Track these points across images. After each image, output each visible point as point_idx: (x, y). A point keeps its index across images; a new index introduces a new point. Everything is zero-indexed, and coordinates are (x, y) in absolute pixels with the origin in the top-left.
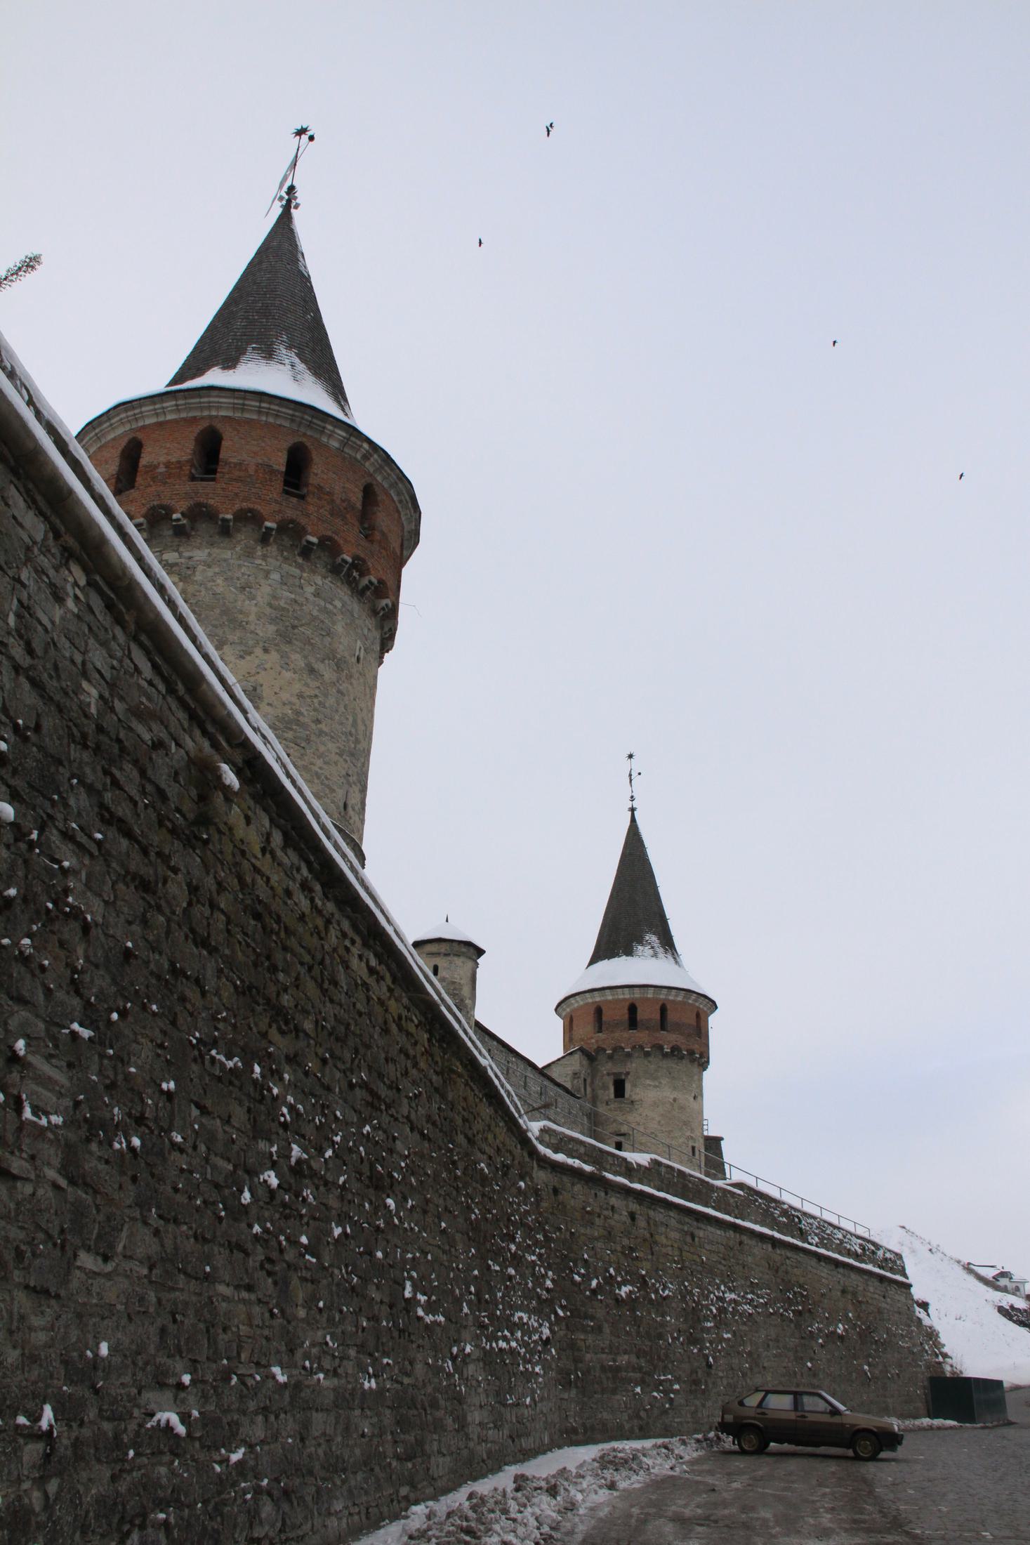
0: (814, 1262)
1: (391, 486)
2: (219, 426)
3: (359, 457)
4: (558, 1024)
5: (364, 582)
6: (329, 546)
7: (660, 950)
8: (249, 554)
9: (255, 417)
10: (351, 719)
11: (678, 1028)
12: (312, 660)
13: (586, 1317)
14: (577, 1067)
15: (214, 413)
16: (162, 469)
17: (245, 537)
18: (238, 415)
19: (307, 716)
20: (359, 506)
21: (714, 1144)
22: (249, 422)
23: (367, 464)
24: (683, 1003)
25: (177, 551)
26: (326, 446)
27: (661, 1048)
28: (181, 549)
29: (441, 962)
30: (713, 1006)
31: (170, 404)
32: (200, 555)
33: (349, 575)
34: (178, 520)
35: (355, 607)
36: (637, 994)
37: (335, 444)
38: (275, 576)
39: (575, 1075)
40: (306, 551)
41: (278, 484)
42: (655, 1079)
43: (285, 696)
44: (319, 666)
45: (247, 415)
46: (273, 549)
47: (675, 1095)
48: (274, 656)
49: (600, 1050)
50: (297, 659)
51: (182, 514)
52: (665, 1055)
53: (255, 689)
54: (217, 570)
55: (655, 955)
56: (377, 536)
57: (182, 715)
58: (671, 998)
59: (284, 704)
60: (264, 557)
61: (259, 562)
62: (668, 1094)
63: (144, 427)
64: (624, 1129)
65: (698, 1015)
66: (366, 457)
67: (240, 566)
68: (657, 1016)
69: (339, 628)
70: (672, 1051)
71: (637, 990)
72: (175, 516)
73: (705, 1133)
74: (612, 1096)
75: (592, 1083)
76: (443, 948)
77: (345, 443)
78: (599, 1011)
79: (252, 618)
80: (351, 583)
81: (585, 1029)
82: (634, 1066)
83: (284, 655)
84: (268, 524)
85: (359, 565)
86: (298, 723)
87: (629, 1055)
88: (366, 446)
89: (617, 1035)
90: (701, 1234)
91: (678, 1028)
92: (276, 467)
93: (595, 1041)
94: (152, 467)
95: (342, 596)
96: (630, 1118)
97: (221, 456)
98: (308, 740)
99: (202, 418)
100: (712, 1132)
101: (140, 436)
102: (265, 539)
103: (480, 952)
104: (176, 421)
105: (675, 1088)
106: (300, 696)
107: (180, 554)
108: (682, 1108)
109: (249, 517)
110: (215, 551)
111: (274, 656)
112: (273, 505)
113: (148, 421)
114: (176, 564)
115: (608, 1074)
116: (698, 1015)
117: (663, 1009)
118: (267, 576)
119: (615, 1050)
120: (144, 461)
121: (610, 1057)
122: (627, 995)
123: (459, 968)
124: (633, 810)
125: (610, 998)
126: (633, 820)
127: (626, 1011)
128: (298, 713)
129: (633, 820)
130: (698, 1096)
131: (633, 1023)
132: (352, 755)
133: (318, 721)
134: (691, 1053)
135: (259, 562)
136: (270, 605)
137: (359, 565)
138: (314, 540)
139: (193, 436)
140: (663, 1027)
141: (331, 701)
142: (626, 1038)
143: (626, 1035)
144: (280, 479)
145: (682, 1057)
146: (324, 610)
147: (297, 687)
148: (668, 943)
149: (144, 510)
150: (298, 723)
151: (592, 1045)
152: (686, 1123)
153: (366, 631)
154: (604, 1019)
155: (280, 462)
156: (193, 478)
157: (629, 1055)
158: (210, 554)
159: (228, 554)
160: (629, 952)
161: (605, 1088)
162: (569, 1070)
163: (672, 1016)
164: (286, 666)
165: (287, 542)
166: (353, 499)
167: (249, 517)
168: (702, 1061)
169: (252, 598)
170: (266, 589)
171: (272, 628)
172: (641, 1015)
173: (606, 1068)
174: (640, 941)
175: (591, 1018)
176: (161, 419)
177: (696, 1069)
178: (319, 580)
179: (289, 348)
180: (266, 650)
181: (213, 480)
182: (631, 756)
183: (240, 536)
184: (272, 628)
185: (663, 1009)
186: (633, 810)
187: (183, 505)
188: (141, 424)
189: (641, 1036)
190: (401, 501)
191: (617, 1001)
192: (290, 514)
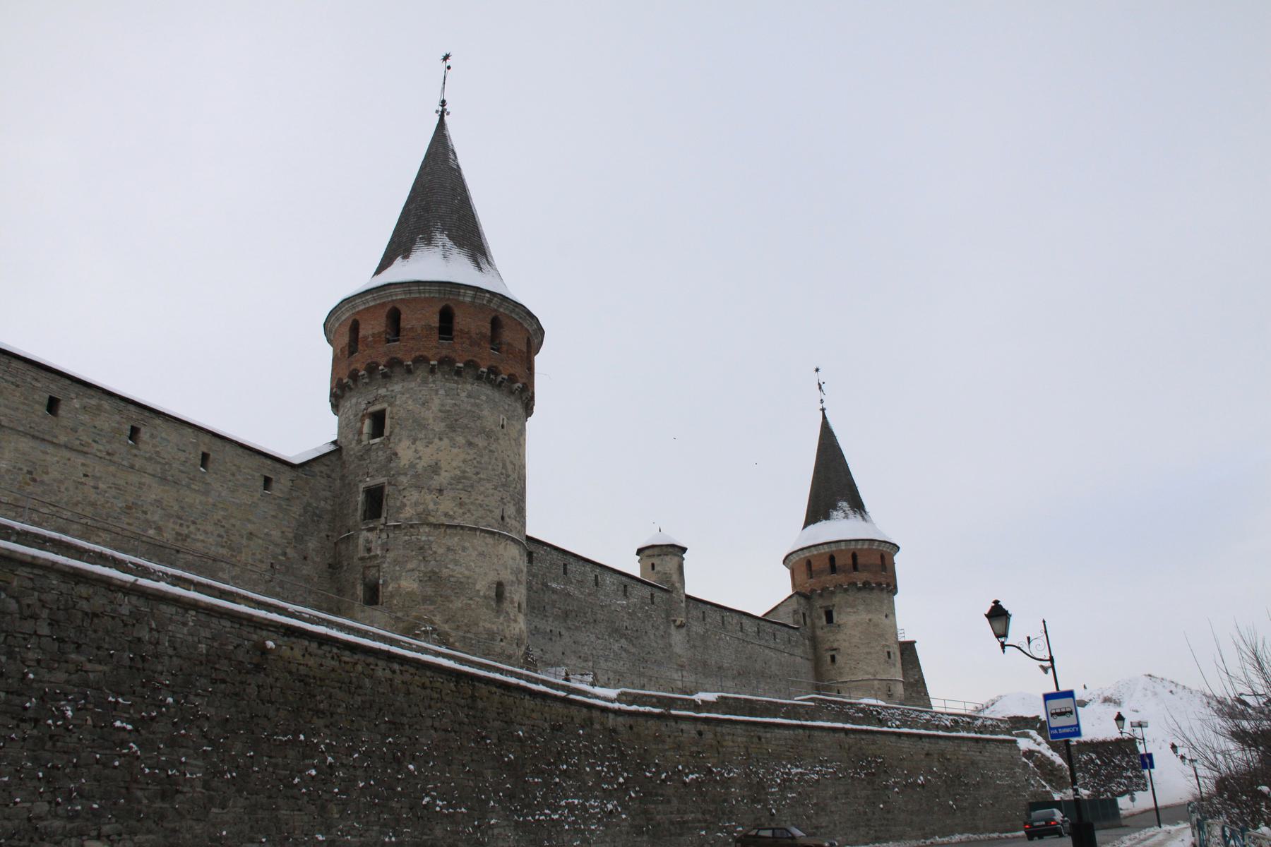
0: (893, 739)
2: (398, 306)
4: (787, 572)
5: (499, 379)
6: (472, 365)
7: (850, 512)
8: (425, 382)
11: (867, 568)
12: (470, 438)
13: (657, 795)
14: (795, 606)
17: (421, 373)
19: (470, 472)
20: (489, 333)
21: (908, 650)
22: (415, 299)
24: (869, 550)
26: (463, 302)
29: (656, 561)
32: (397, 388)
33: (488, 377)
35: (496, 395)
36: (834, 548)
37: (468, 299)
38: (442, 392)
39: (795, 612)
40: (458, 372)
41: (436, 335)
42: (853, 607)
43: (454, 464)
44: (475, 440)
46: (439, 375)
47: (870, 616)
48: (446, 441)
49: (813, 591)
50: (461, 440)
52: (859, 589)
55: (846, 517)
56: (505, 348)
57: (252, 630)
60: (434, 382)
62: (865, 617)
63: (358, 312)
64: (835, 645)
65: (882, 557)
66: (490, 301)
68: (850, 562)
69: (486, 413)
73: (901, 639)
74: (824, 622)
75: (810, 616)
76: (656, 551)
78: (809, 563)
79: (431, 421)
80: (490, 382)
81: (802, 576)
82: (838, 599)
83: (452, 439)
85: (493, 370)
86: (465, 478)
87: (833, 593)
89: (823, 578)
90: (768, 735)
91: (867, 568)
93: (809, 584)
94: (366, 337)
95: (486, 391)
96: (839, 637)
97: (402, 324)
98: (472, 486)
100: (904, 637)
101: (357, 317)
102: (432, 370)
103: (684, 550)
104: (375, 307)
105: (869, 612)
106: (464, 461)
108: (876, 625)
109: (421, 360)
110: (406, 384)
111: (446, 441)
112: (434, 349)
116: (882, 557)
117: (854, 556)
120: (361, 335)
121: (821, 595)
122: (826, 549)
123: (669, 563)
124: (823, 410)
126: (824, 417)
128: (464, 472)
129: (824, 417)
130: (890, 613)
131: (833, 569)
132: (503, 485)
133: (477, 473)
134: (879, 584)
137: (493, 370)
139: (384, 315)
140: (855, 568)
141: (486, 459)
142: (830, 580)
143: (829, 578)
144: (437, 331)
145: (873, 589)
146: (477, 405)
147: (462, 456)
148: (857, 506)
150: (465, 478)
151: (806, 590)
152: (881, 636)
155: (435, 321)
156: (388, 341)
157: (833, 593)
159: (413, 385)
160: (827, 517)
161: (820, 618)
162: (790, 609)
163: (860, 560)
164: (454, 446)
165: (446, 368)
166: (484, 331)
167: (421, 360)
168: (890, 588)
170: (437, 401)
172: (839, 562)
173: (819, 603)
174: (835, 508)
175: (804, 568)
177: (885, 595)
178: (469, 387)
179: (442, 232)
180: (441, 439)
182: (817, 370)
183: (418, 372)
185: (854, 556)
186: (823, 410)
187: (383, 360)
189: (839, 578)
191: (820, 555)
192: (444, 352)
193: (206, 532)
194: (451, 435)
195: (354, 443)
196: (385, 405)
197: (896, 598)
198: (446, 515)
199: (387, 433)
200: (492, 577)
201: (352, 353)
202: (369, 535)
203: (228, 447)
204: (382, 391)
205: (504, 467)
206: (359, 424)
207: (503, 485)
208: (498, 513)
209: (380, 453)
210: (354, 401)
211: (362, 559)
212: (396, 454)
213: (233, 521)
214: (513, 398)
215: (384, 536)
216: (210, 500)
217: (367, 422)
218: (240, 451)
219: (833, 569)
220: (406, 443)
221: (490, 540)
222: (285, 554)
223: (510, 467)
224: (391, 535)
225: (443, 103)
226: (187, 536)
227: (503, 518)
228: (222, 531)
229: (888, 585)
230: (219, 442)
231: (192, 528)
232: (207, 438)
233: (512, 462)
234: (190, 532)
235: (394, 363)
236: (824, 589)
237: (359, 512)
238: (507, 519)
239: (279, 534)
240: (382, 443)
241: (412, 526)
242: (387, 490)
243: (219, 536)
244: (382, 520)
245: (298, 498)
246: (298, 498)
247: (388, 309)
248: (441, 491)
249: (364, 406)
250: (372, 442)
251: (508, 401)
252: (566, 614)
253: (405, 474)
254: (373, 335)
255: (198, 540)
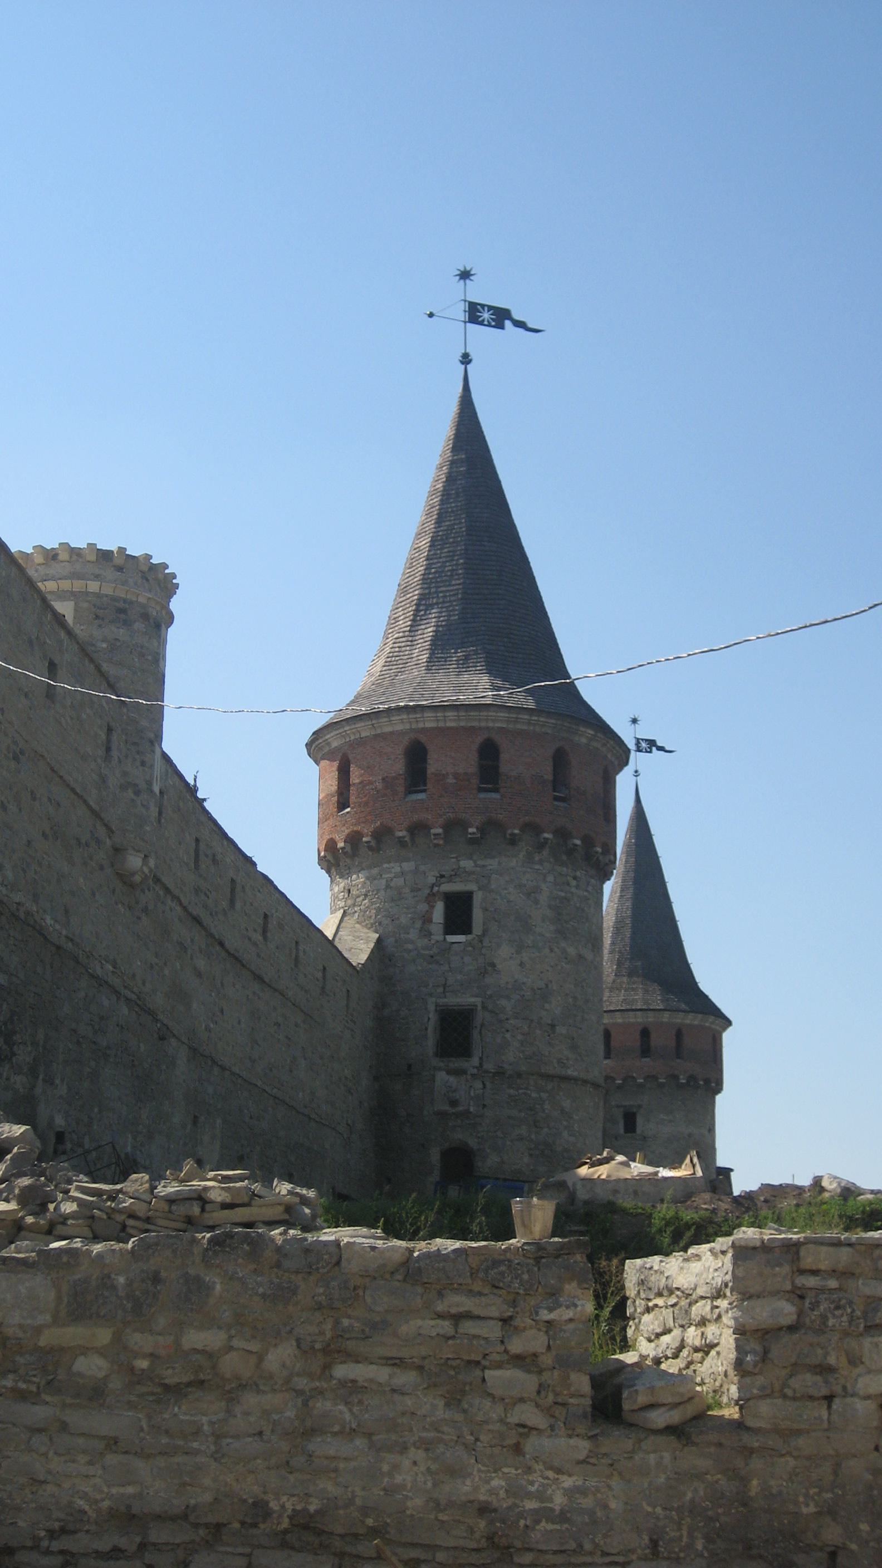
9: (525, 727)
15: (491, 724)
16: (451, 780)
18: (511, 726)
25: (471, 859)
27: (675, 1077)
28: (475, 858)
30: (728, 1023)
31: (450, 714)
32: (492, 863)
34: (474, 833)
37: (584, 740)
38: (550, 878)
40: (571, 852)
45: (519, 726)
46: (546, 852)
51: (477, 828)
52: (681, 1086)
53: (547, 986)
54: (507, 878)
58: (688, 1022)
59: (567, 995)
61: (537, 867)
63: (424, 731)
67: (524, 873)
70: (688, 1083)
71: (650, 1014)
72: (470, 830)
74: (622, 1131)
84: (546, 835)
92: (546, 777)
97: (504, 768)
99: (480, 728)
100: (721, 1162)
101: (423, 739)
102: (541, 846)
107: (475, 862)
113: (428, 725)
114: (473, 873)
115: (618, 1106)
117: (679, 1034)
118: (545, 881)
119: (625, 1080)
120: (432, 768)
125: (620, 1021)
127: (638, 1037)
128: (575, 998)
131: (646, 1051)
135: (537, 867)
136: (550, 907)
138: (578, 842)
140: (679, 1055)
149: (441, 821)
154: (613, 1044)
156: (480, 790)
157: (641, 1085)
158: (500, 864)
159: (513, 863)
169: (536, 902)
171: (552, 928)
172: (656, 1040)
176: (441, 724)
181: (496, 790)
182: (634, 721)
184: (552, 928)
185: (679, 1034)
188: (421, 725)
194: (563, 944)
195: (413, 935)
196: (471, 887)
197: (718, 1098)
198: (559, 1061)
199: (477, 928)
201: (410, 791)
202: (452, 1080)
204: (467, 864)
206: (423, 907)
209: (467, 959)
210: (408, 866)
211: (442, 1115)
212: (493, 965)
215: (478, 1085)
217: (440, 907)
219: (646, 1051)
220: (505, 951)
224: (488, 1085)
225: (466, 359)
229: (707, 1081)
235: (491, 827)
236: (628, 1078)
237: (430, 1043)
240: (469, 944)
241: (519, 1075)
242: (480, 1016)
244: (475, 1061)
247: (479, 739)
248: (553, 1026)
249: (431, 880)
250: (451, 938)
253: (508, 998)
254: (456, 776)
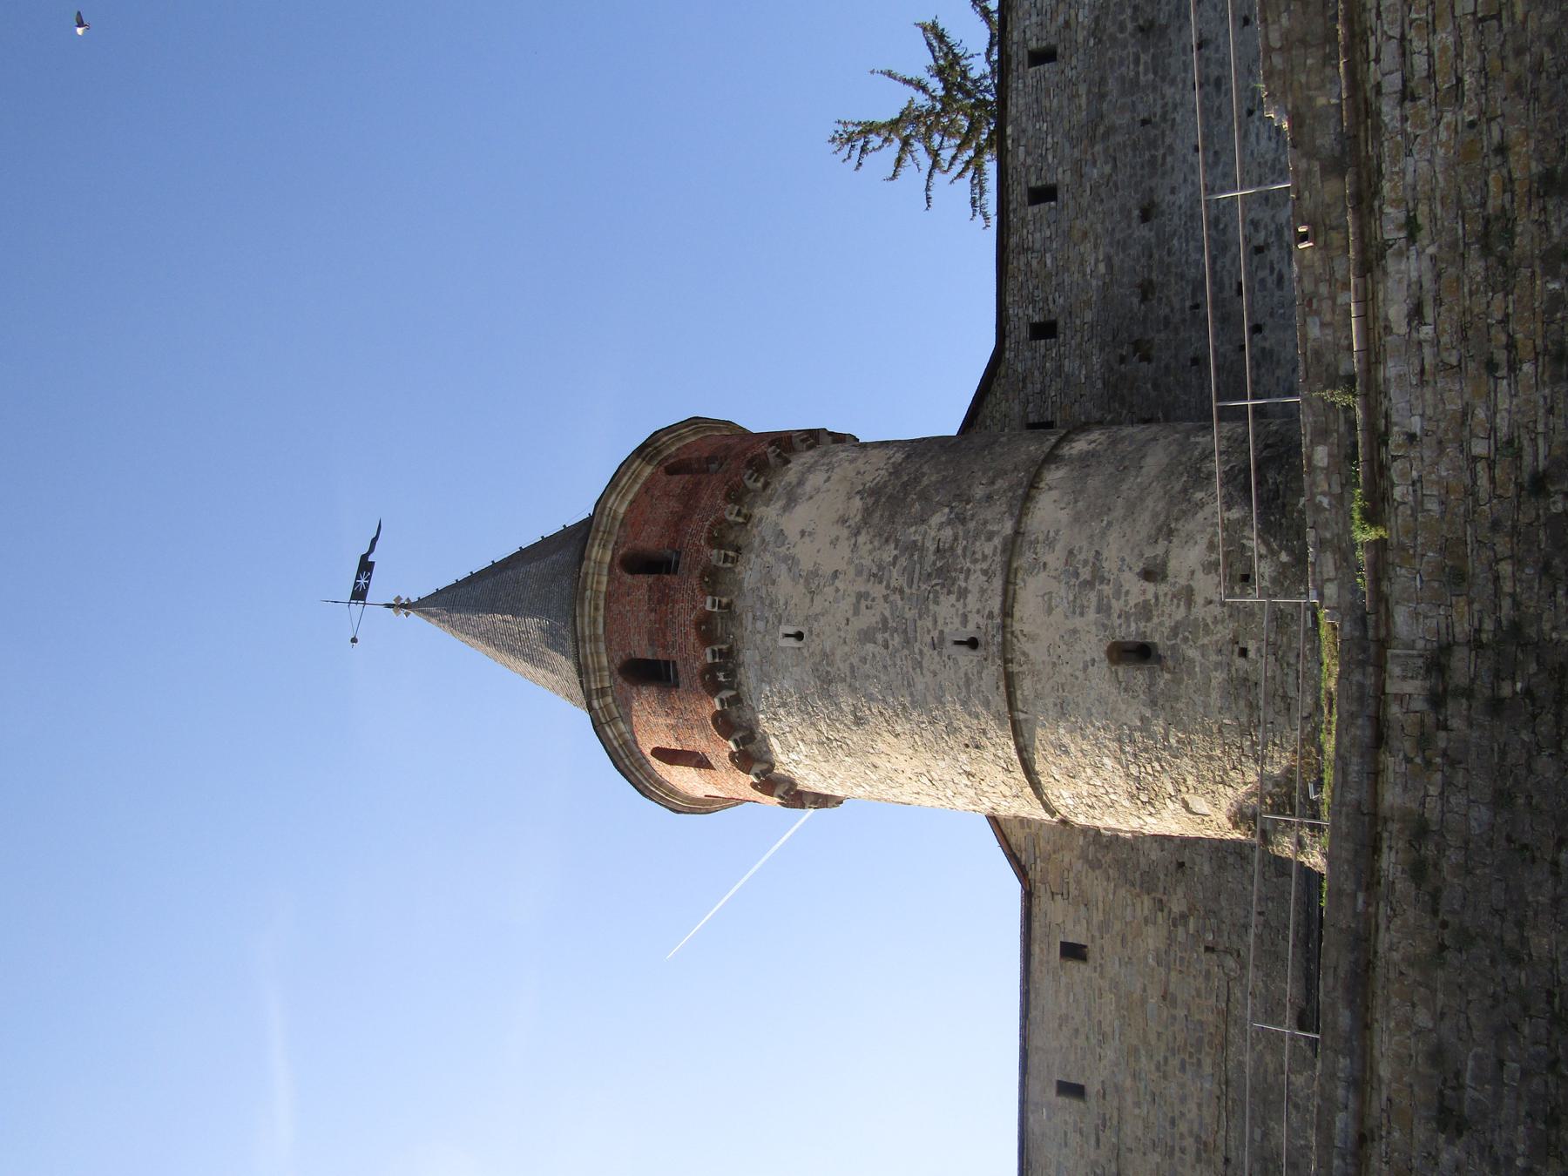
1: (596, 639)
3: (610, 699)
10: (870, 647)
23: (607, 684)
35: (748, 656)
66: (602, 693)
77: (612, 721)
88: (595, 704)
153: (760, 625)
190: (596, 609)
193: (1183, 1100)
200: (1101, 678)
203: (1036, 1041)
205: (867, 636)
207: (907, 642)
208: (966, 658)
213: (1152, 1038)
214: (739, 606)
216: (1128, 1083)
218: (1033, 1013)
221: (1026, 688)
222: (1184, 917)
223: (868, 619)
226: (1198, 1138)
227: (973, 643)
228: (1175, 1062)
230: (1034, 1060)
231: (1183, 1127)
232: (1035, 1087)
233: (856, 612)
234: (1191, 1132)
238: (970, 631)
239: (1151, 929)
243: (1183, 1063)
245: (1078, 882)
246: (1078, 882)
248: (968, 774)
251: (748, 619)
252: (1147, 30)
255: (1201, 1117)
